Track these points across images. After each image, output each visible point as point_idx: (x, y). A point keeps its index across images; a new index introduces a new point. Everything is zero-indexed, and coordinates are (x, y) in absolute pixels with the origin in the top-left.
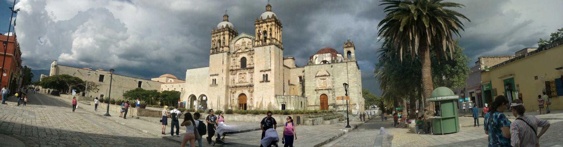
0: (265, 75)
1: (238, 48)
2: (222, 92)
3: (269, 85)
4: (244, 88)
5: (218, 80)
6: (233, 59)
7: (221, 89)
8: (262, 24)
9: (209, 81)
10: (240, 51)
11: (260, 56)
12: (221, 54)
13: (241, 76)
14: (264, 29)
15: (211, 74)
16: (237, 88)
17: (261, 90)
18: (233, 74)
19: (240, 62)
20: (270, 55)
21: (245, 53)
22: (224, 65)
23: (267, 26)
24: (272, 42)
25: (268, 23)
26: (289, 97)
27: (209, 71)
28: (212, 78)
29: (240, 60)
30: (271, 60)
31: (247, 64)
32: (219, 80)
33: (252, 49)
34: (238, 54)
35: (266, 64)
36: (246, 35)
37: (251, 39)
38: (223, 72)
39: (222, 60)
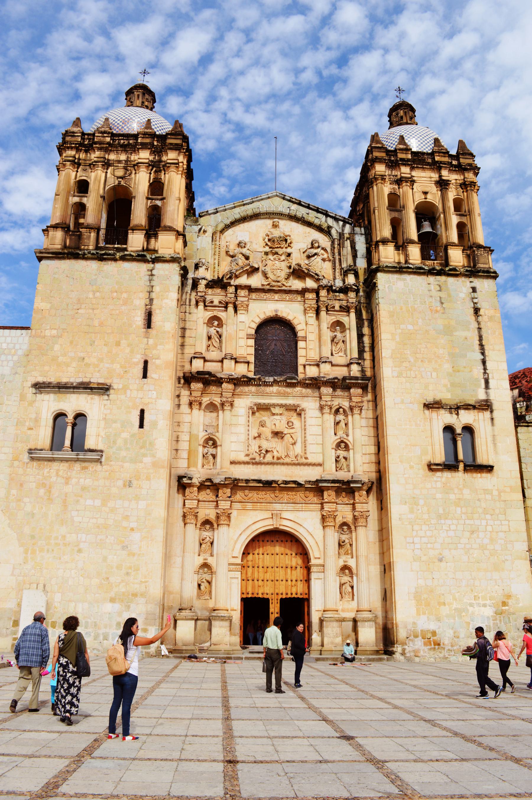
1: (241, 261)
3: (486, 491)
4: (285, 496)
6: (209, 314)
7: (129, 484)
8: (412, 168)
9: (19, 423)
10: (256, 281)
11: (420, 320)
12: (143, 268)
13: (262, 425)
14: (426, 193)
15: (41, 379)
16: (239, 495)
17: (439, 517)
18: (206, 400)
19: (252, 342)
21: (287, 297)
23: (443, 184)
24: (482, 266)
25: (445, 173)
29: (253, 332)
30: (483, 354)
31: (301, 361)
33: (339, 283)
34: (242, 293)
35: (456, 370)
36: (294, 207)
38: (145, 376)
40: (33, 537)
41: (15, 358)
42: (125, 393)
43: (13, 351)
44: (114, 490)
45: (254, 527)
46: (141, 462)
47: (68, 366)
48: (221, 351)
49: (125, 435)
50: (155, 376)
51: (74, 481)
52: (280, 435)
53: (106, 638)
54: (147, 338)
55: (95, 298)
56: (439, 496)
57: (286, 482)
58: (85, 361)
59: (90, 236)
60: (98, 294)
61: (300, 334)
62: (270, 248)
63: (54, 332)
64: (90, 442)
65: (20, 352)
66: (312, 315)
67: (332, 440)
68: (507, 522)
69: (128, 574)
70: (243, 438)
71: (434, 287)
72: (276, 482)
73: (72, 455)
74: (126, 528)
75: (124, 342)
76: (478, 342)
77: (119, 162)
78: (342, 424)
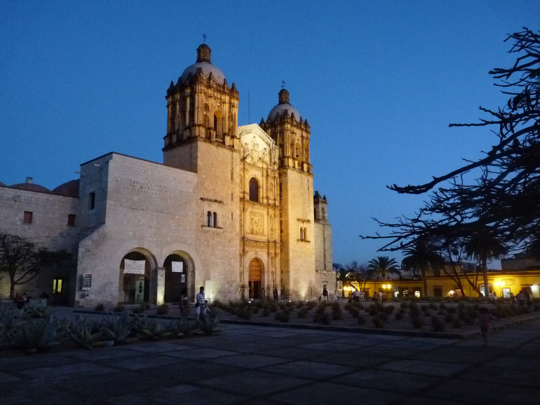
0: (304, 229)
2: (234, 248)
3: (308, 249)
5: (224, 217)
7: (230, 242)
9: (197, 214)
15: (203, 197)
20: (308, 194)
22: (234, 182)
23: (302, 136)
26: (330, 272)
27: (197, 184)
28: (207, 207)
31: (261, 196)
32: (226, 218)
37: (269, 146)
38: (232, 200)
39: (229, 168)
40: (204, 260)
41: (194, 186)
42: (227, 206)
43: (193, 182)
44: (226, 243)
45: (251, 257)
46: (233, 233)
47: (210, 192)
48: (242, 189)
49: (228, 223)
50: (235, 200)
51: (215, 239)
52: (257, 224)
53: (226, 297)
54: (232, 184)
55: (216, 163)
56: (299, 250)
57: (261, 242)
58: (215, 191)
59: (213, 134)
60: (217, 162)
61: (261, 185)
62: (253, 147)
63: (205, 176)
64: (219, 224)
65: (195, 184)
66: (264, 179)
67: (270, 227)
68: (311, 259)
69: (231, 274)
70: (248, 224)
71: (300, 178)
72: (258, 241)
73: (215, 229)
74: (230, 257)
75: (226, 184)
76: (308, 200)
77: (218, 98)
78: (272, 222)
